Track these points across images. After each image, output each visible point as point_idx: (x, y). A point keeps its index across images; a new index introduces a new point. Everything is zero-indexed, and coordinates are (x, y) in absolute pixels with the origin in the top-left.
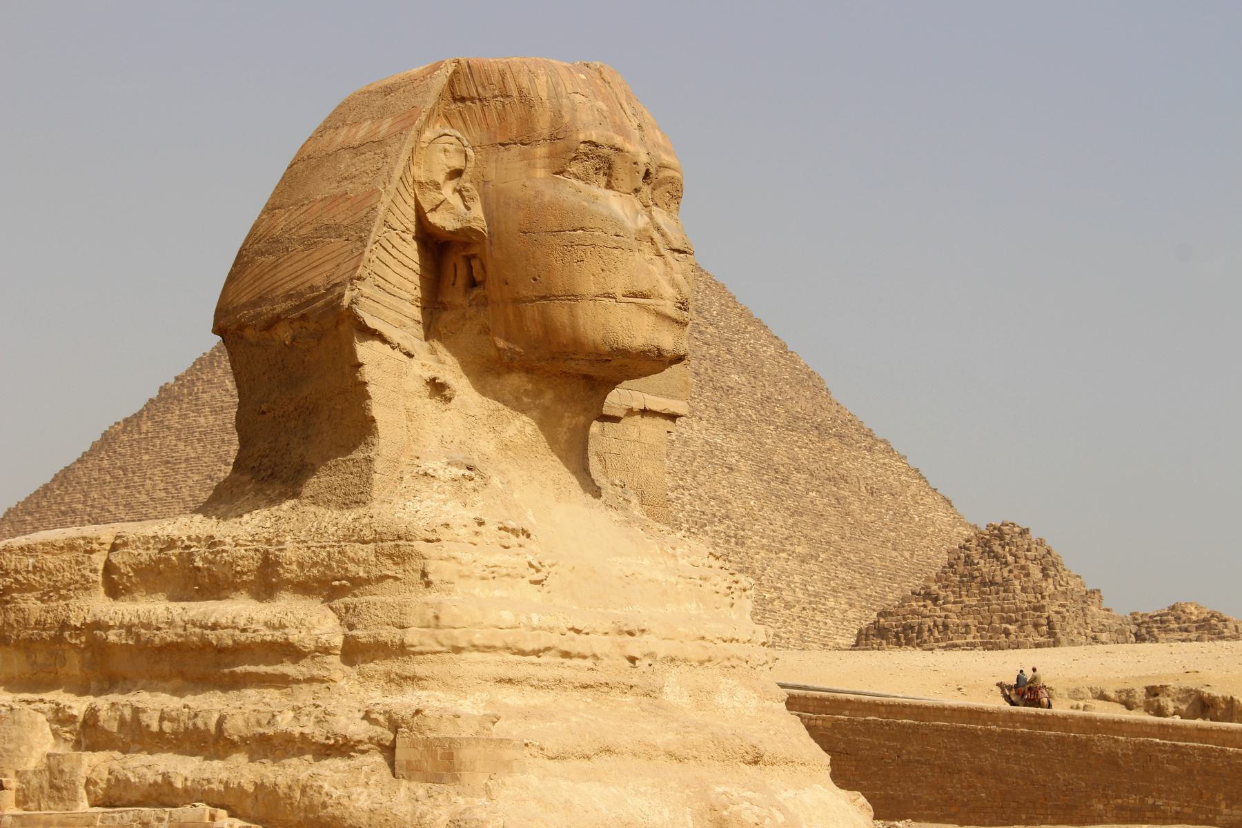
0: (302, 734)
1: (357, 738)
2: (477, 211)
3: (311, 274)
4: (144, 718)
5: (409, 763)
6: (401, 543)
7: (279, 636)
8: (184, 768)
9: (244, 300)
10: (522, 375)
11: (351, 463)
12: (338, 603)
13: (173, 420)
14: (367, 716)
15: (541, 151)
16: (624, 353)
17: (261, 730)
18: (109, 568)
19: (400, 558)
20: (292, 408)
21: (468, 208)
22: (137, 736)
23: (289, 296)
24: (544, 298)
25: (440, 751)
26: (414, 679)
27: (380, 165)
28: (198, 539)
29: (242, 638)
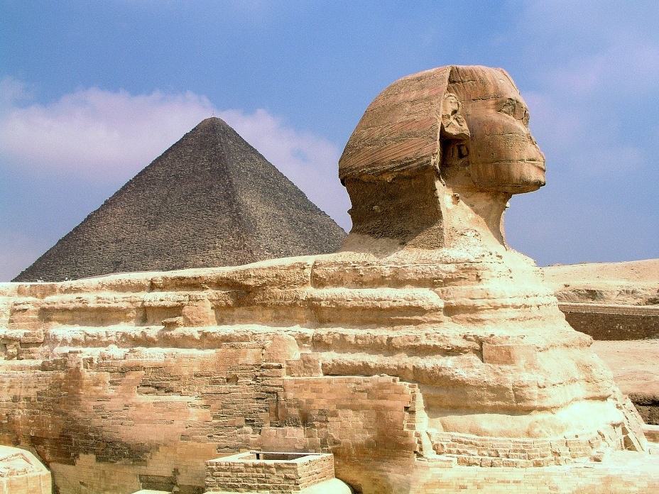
2: (465, 126)
4: (347, 338)
7: (413, 304)
8: (373, 360)
12: (438, 289)
13: (110, 211)
14: (465, 337)
15: (491, 102)
16: (528, 183)
18: (314, 276)
22: (342, 344)
23: (392, 162)
25: (504, 352)
28: (358, 263)
29: (395, 304)
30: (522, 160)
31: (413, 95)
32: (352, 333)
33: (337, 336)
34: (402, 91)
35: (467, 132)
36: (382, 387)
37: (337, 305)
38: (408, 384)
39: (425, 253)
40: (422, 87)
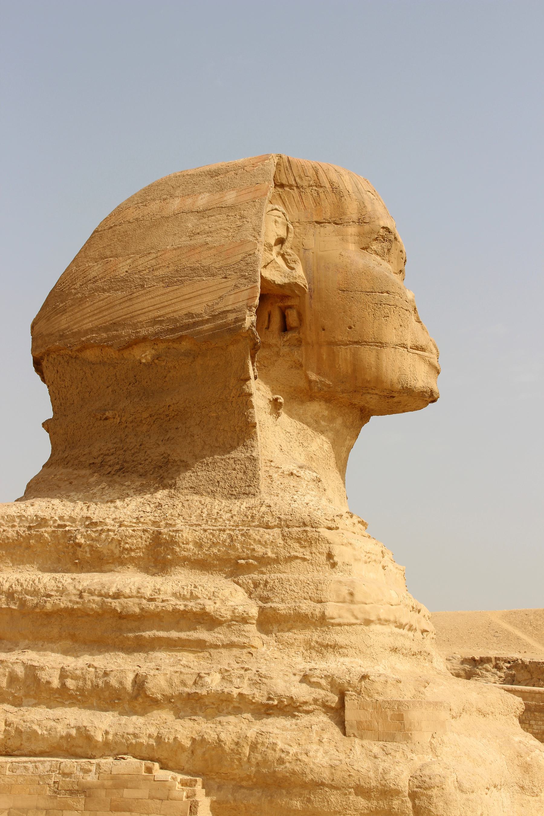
0: (240, 694)
1: (302, 699)
2: (300, 271)
3: (184, 305)
5: (359, 723)
6: (308, 529)
8: (103, 723)
9: (90, 325)
10: (322, 403)
11: (232, 461)
14: (305, 679)
15: (352, 230)
17: (187, 690)
19: (307, 542)
20: (145, 415)
21: (292, 269)
23: (155, 321)
24: (356, 343)
25: (389, 713)
26: (335, 647)
27: (239, 223)
29: (152, 606)
30: (404, 346)
31: (203, 200)
32: (51, 663)
33: (20, 671)
34: (178, 192)
35: (303, 282)
36: (119, 783)
37: (23, 603)
38: (180, 777)
39: (219, 505)
40: (221, 188)
